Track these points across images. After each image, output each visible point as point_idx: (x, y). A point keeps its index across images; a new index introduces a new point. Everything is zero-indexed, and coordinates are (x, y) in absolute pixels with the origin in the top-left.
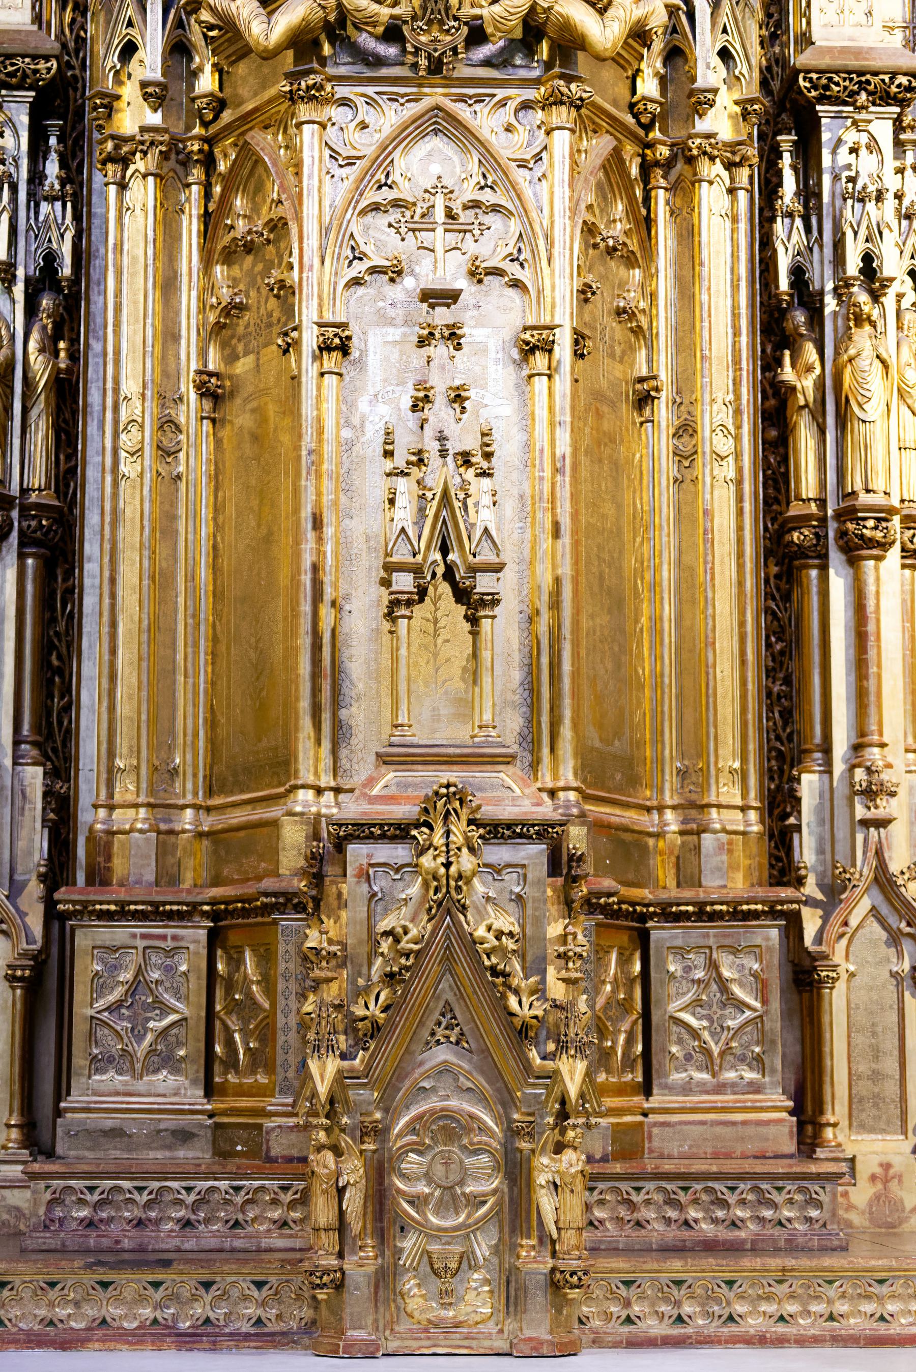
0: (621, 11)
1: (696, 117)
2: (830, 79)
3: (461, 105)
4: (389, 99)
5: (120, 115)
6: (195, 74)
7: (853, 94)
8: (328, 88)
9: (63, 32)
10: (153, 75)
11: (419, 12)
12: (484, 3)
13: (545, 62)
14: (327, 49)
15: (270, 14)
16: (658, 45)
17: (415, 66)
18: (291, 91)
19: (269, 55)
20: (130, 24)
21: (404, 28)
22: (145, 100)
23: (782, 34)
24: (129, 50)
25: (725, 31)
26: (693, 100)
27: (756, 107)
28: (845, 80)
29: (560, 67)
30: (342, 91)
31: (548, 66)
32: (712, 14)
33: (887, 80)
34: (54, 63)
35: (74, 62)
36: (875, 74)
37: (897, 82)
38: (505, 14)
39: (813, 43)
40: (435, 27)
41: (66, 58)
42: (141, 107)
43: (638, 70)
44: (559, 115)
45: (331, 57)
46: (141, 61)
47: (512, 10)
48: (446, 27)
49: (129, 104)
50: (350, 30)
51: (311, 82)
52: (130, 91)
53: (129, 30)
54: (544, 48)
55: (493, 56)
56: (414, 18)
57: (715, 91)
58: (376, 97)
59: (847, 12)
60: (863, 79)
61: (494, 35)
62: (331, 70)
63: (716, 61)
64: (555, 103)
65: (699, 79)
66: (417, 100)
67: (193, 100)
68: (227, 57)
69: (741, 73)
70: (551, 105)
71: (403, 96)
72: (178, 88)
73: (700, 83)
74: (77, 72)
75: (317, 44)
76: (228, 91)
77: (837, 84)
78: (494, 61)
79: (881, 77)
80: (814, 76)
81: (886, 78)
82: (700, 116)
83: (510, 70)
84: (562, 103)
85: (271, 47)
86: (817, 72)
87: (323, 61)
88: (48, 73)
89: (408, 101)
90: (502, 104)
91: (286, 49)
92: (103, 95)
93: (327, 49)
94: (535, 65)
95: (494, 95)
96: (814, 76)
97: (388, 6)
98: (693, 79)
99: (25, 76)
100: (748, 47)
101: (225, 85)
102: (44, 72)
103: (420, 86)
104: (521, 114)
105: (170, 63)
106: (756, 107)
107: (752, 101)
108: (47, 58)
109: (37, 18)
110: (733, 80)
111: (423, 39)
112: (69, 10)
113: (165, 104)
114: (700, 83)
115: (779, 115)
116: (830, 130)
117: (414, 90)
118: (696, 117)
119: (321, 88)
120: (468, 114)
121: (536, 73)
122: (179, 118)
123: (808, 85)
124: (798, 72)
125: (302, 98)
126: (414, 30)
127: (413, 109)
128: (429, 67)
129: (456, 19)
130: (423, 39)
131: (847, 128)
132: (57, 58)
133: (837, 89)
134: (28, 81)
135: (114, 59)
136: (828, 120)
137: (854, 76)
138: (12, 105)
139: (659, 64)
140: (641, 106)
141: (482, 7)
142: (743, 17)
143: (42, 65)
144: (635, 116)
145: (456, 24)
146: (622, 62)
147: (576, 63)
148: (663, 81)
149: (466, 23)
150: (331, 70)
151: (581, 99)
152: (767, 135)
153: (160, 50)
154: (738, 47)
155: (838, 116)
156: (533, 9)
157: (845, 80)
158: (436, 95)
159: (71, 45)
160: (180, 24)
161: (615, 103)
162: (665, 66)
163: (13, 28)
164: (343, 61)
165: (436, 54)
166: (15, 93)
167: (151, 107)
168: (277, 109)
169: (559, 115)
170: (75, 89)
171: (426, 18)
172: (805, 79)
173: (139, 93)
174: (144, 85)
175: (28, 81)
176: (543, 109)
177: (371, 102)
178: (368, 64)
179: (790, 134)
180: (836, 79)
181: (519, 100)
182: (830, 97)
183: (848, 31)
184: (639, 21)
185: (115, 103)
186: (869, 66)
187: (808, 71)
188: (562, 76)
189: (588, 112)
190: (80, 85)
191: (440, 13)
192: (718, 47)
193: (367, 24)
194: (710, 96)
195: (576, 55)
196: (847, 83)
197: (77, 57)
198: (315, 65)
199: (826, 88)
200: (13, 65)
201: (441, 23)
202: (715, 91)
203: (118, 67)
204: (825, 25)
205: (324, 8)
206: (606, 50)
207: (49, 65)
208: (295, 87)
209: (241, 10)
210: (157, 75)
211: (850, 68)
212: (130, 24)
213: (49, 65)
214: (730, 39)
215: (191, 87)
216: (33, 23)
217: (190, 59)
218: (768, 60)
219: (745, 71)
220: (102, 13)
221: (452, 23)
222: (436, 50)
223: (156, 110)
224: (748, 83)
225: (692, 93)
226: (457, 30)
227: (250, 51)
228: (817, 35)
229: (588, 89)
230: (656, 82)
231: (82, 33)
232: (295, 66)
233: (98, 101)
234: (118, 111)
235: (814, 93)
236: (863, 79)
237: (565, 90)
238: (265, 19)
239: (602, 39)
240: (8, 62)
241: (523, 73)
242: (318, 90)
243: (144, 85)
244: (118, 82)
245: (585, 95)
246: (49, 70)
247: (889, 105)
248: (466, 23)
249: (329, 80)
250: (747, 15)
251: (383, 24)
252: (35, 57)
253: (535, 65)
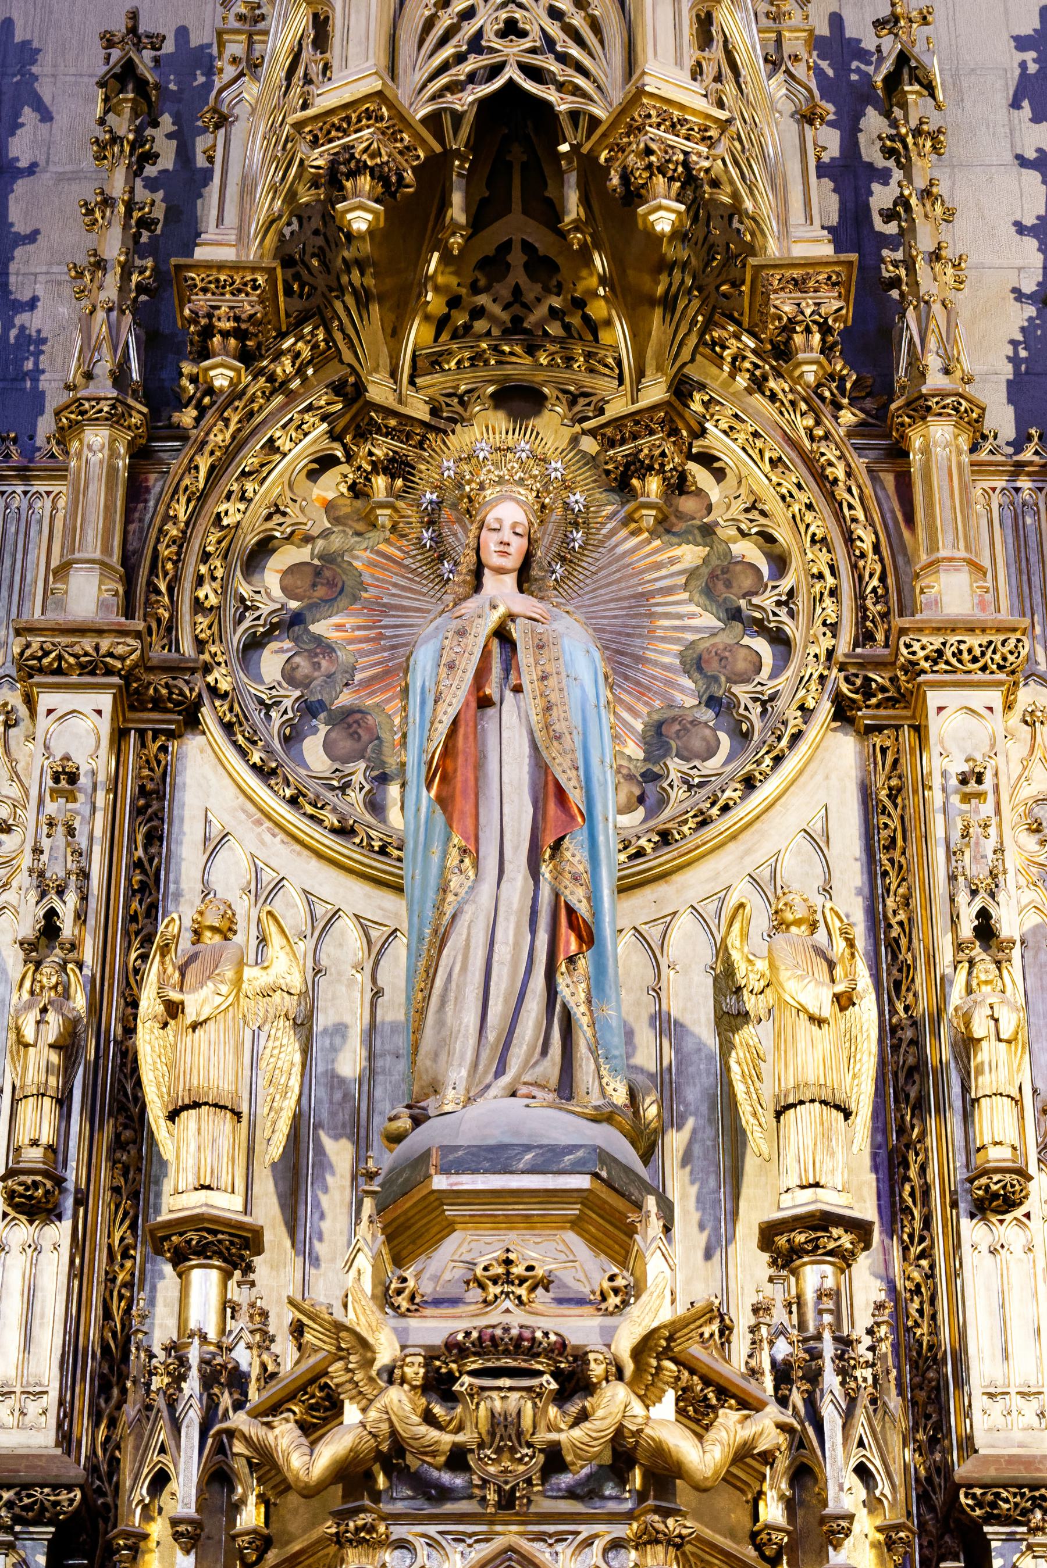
0: (724, 1434)
1: (830, 1549)
2: (997, 1495)
3: (539, 1545)
4: (454, 1540)
5: (147, 1557)
6: (236, 1508)
7: (1025, 1512)
8: (382, 1529)
9: (95, 1453)
10: (186, 1510)
11: (487, 1439)
12: (563, 1426)
13: (638, 1492)
14: (381, 1481)
15: (313, 1444)
16: (782, 1463)
17: (483, 1499)
18: (337, 1533)
19: (311, 1492)
20: (163, 1450)
21: (470, 1457)
22: (176, 1540)
23: (943, 1437)
24: (161, 1480)
25: (861, 1444)
26: (825, 1528)
27: (902, 1534)
28: (1015, 1495)
29: (656, 1498)
30: (399, 1531)
31: (641, 1497)
32: (844, 1426)
34: (78, 1493)
35: (106, 1487)
38: (587, 1439)
39: (976, 1451)
40: (506, 1455)
41: (98, 1483)
42: (173, 1548)
43: (760, 1494)
44: (654, 1556)
45: (386, 1490)
46: (173, 1494)
47: (594, 1435)
48: (518, 1455)
49: (158, 1543)
50: (410, 1459)
51: (360, 1523)
52: (158, 1529)
53: (162, 1458)
54: (637, 1478)
55: (580, 1484)
56: (481, 1446)
57: (851, 1517)
58: (438, 1537)
59: (1014, 1413)
60: (1037, 1494)
61: (574, 1464)
62: (385, 1507)
63: (853, 1480)
64: (649, 1542)
65: (831, 1504)
66: (487, 1540)
67: (234, 1538)
68: (274, 1488)
69: (882, 1494)
70: (645, 1544)
71: (470, 1535)
72: (214, 1526)
73: (831, 1509)
74: (109, 1500)
75: (370, 1477)
76: (274, 1526)
78: (579, 1491)
80: (978, 1491)
82: (835, 1548)
83: (598, 1503)
84: (658, 1542)
85: (312, 1483)
86: (981, 1487)
87: (376, 1496)
88: (70, 1505)
89: (477, 1541)
90: (588, 1543)
91: (331, 1484)
92: (127, 1535)
93: (381, 1481)
94: (627, 1495)
95: (578, 1533)
96: (978, 1491)
97: (451, 1432)
98: (825, 1505)
99: (43, 1509)
100: (890, 1462)
101: (273, 1518)
102: (66, 1504)
103: (492, 1523)
104: (611, 1555)
105: (207, 1496)
106: (902, 1534)
107: (897, 1528)
108: (70, 1488)
109: (65, 1438)
110: (873, 1504)
111: (492, 1469)
112: (103, 1426)
113: (199, 1544)
114: (831, 1509)
115: (942, 1537)
116: (1002, 1556)
117: (484, 1528)
118: (830, 1549)
119: (371, 1529)
120: (547, 1555)
121: (629, 1505)
122: (217, 1561)
123: (970, 1502)
124: (959, 1486)
125: (350, 1541)
126: (480, 1459)
127: (485, 1550)
128: (499, 1502)
129: (529, 1445)
130: (492, 1469)
131: (1023, 1554)
132: (82, 1487)
133: (1007, 1506)
134: (47, 1515)
135: (143, 1491)
136: (998, 1544)
137: (1025, 1490)
138: (28, 1543)
139: (784, 1485)
140: (764, 1536)
141: (560, 1430)
142: (883, 1427)
143: (64, 1496)
144: (758, 1548)
145: (530, 1452)
146: (739, 1484)
147: (674, 1494)
148: (791, 1506)
149: (541, 1451)
150: (385, 1507)
151: (680, 1536)
152: (930, 1560)
153: (195, 1479)
154: (878, 1462)
155: (1010, 1538)
156: (620, 1431)
157: (1015, 1495)
158: (510, 1535)
159: (104, 1468)
160: (221, 1449)
161: (732, 1535)
162: (791, 1486)
163: (33, 1452)
164: (400, 1496)
165: (507, 1487)
166: (32, 1529)
167: (182, 1549)
168: (326, 1551)
169: (654, 1556)
170: (106, 1520)
171: (495, 1445)
172: (966, 1495)
173: (170, 1531)
174: (175, 1522)
175: (47, 1515)
176: (637, 1549)
177: (433, 1543)
178: (429, 1498)
179: (959, 1561)
180: (1005, 1494)
181: (608, 1538)
182: (999, 1516)
183: (1018, 1436)
184: (745, 1443)
185: (142, 1544)
187: (970, 1486)
188: (657, 1510)
189: (694, 1549)
190: (111, 1515)
191: (510, 1440)
192: (853, 1463)
193: (425, 1454)
194: (844, 1524)
195: (674, 1484)
196: (1018, 1499)
197: (110, 1482)
198: (367, 1502)
199: (993, 1505)
200: (29, 1496)
201: (513, 1450)
202: (851, 1517)
203: (147, 1501)
204: (990, 1430)
205: (375, 1436)
206: (706, 1479)
207: (72, 1495)
208: (342, 1528)
209: (280, 1440)
210: (191, 1511)
211: (1020, 1482)
212: (163, 1450)
213: (72, 1495)
214: (868, 1454)
215: (232, 1522)
216: (58, 1444)
217: (232, 1490)
218: (927, 1470)
219: (887, 1492)
220: (131, 1438)
221: (525, 1451)
222: (506, 1482)
223: (188, 1552)
224: (892, 1506)
225: (823, 1520)
226: (532, 1458)
227: (289, 1488)
228: (980, 1440)
229: (688, 1524)
230: (781, 1506)
231: (117, 1453)
232: (344, 1503)
233: (121, 1542)
234: (144, 1553)
235: (978, 1512)
236: (1037, 1494)
237: (661, 1527)
238: (307, 1450)
239: (701, 1467)
240: (24, 1493)
241: (612, 1506)
242: (369, 1532)
243: (175, 1522)
244: (147, 1517)
245: (685, 1532)
246: (71, 1501)
248: (541, 1451)
249: (383, 1518)
250: (887, 1425)
251: (444, 1453)
252: (55, 1487)
253: (627, 1495)
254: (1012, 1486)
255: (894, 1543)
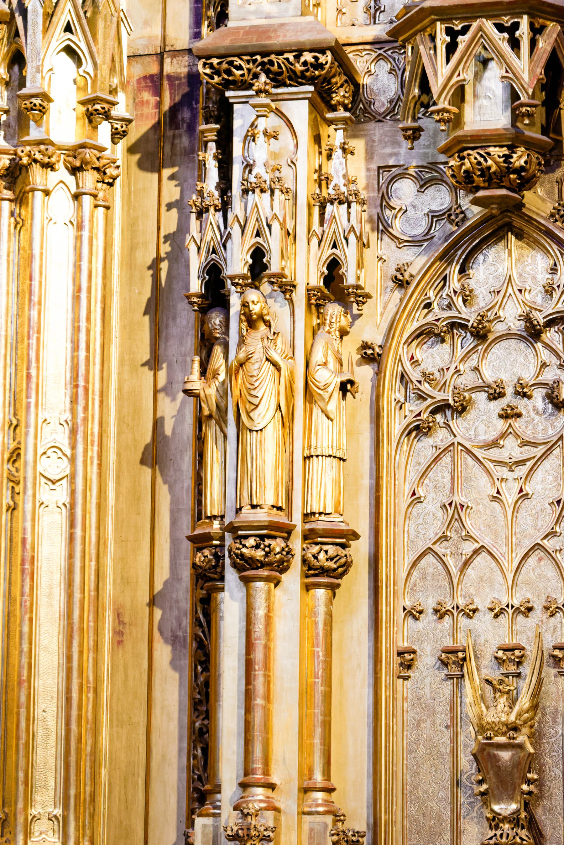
2: (231, 63)
33: (292, 59)
36: (280, 53)
37: (302, 59)
60: (266, 60)
65: (28, 84)
77: (240, 68)
79: (286, 55)
80: (215, 61)
81: (291, 56)
86: (218, 57)
96: (215, 61)
133: (240, 72)
157: (248, 62)
180: (238, 62)
186: (270, 45)
196: (251, 66)
211: (250, 50)
235: (217, 79)
247: (301, 84)
254: (245, 55)
255: (92, 114)
